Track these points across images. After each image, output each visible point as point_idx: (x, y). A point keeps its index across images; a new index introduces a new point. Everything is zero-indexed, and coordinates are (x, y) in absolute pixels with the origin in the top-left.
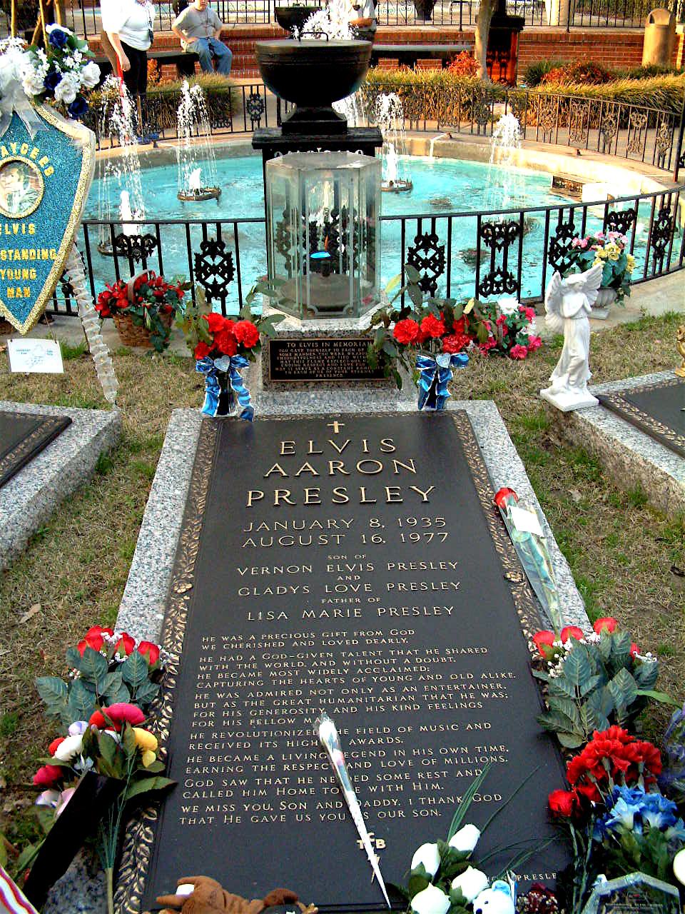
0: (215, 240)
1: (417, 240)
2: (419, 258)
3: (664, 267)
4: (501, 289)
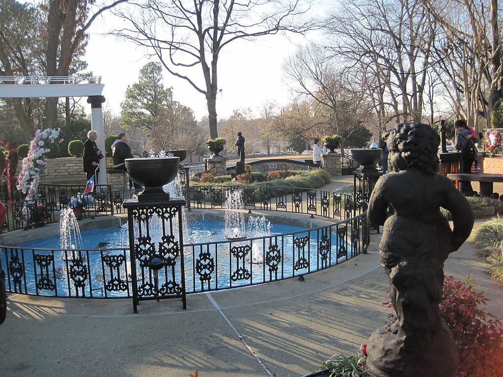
1: (200, 256)
3: (328, 264)
4: (242, 277)
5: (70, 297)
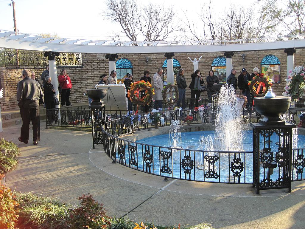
0: (188, 156)
2: (235, 166)
5: (181, 179)
